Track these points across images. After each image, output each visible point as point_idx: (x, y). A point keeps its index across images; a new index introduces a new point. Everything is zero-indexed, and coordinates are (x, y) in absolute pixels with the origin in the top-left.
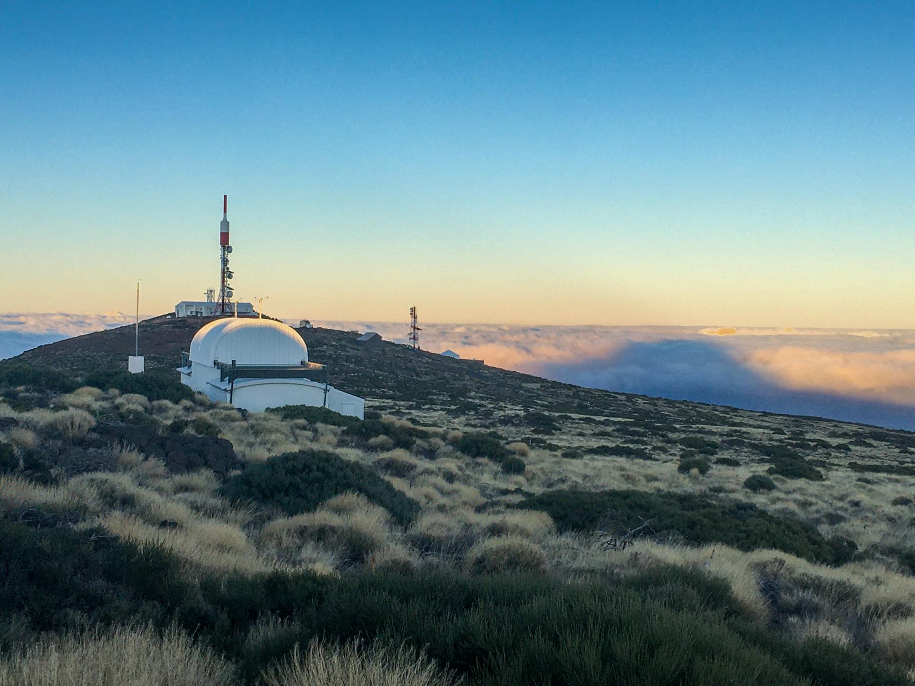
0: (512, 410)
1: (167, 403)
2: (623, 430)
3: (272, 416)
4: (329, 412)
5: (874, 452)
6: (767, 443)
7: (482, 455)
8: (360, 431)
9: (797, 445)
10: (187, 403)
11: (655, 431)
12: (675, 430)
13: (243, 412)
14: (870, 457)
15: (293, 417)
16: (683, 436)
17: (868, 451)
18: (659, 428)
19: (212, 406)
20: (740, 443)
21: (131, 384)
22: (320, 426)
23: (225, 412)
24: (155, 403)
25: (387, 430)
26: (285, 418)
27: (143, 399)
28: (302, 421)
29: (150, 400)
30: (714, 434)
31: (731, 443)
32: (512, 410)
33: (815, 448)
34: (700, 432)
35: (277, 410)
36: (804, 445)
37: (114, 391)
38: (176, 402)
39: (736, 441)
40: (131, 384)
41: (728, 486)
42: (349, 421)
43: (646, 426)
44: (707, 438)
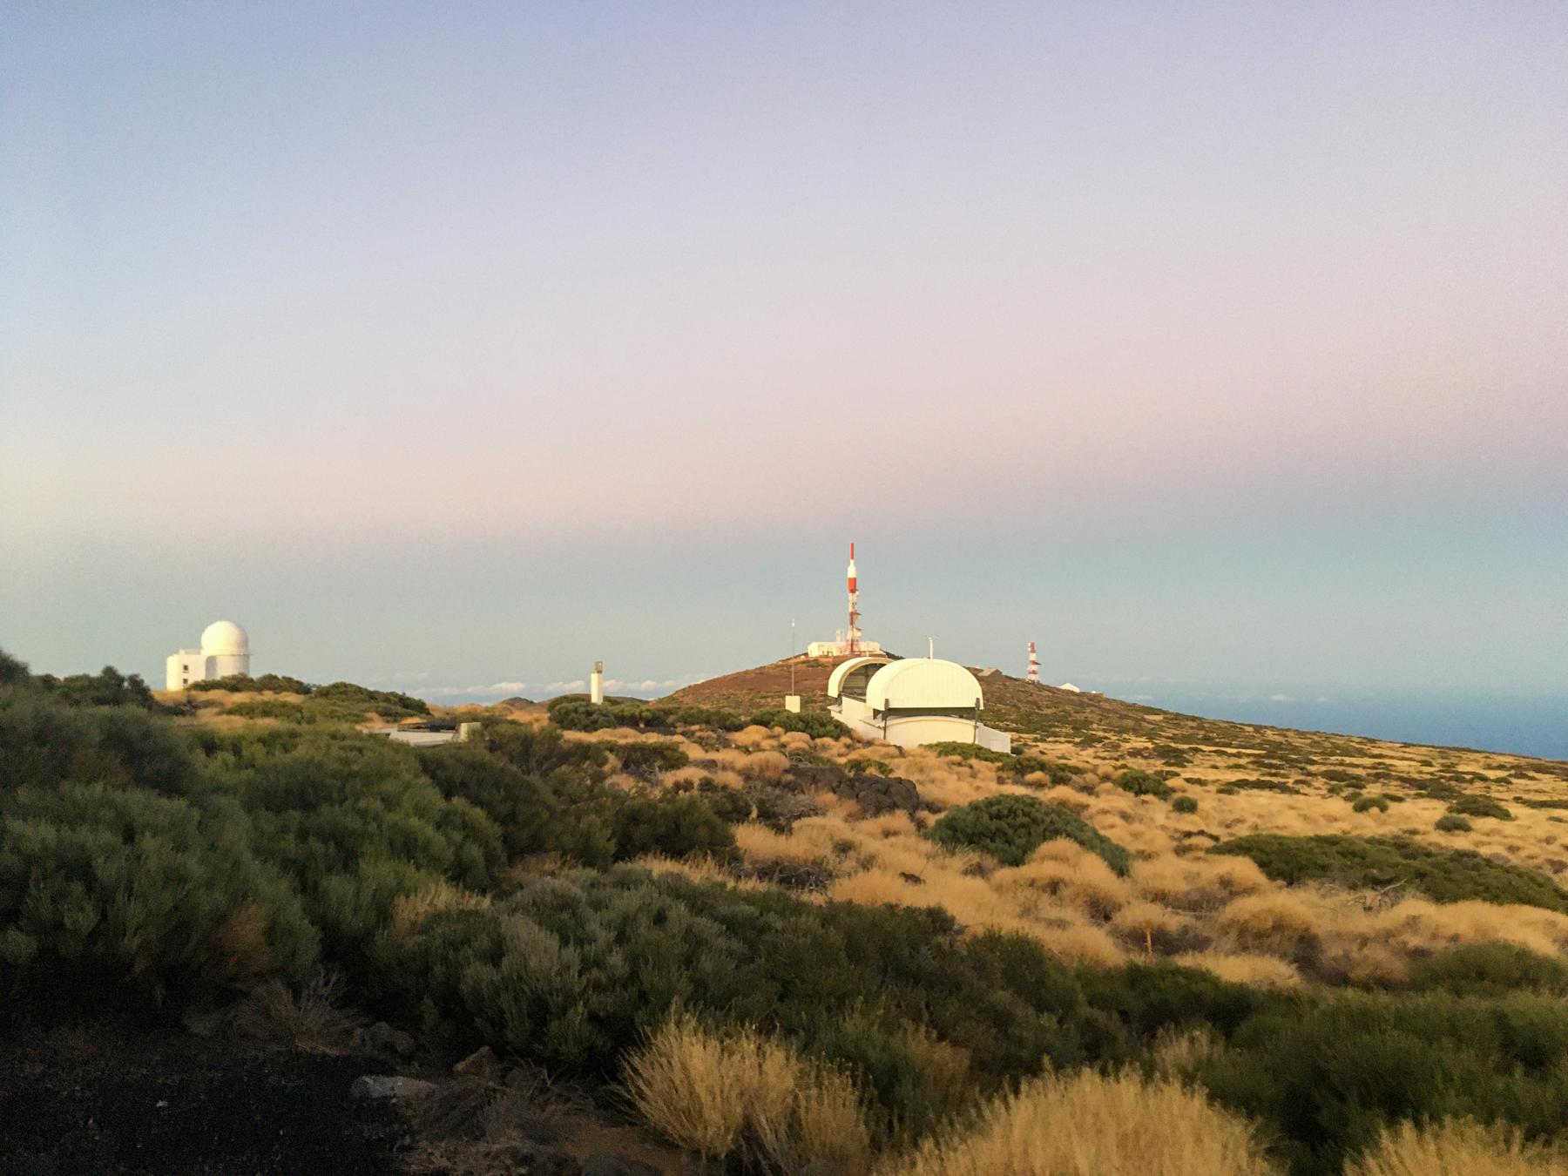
0: (1140, 743)
1: (828, 740)
2: (1258, 762)
3: (928, 753)
4: (980, 748)
5: (1540, 786)
6: (1416, 776)
7: (1146, 792)
8: (1017, 765)
9: (1451, 779)
10: (845, 740)
11: (1292, 764)
12: (1313, 763)
13: (899, 748)
14: (1536, 791)
15: (947, 754)
16: (1324, 768)
17: (1531, 785)
18: (1297, 761)
19: (869, 743)
20: (1387, 776)
21: (791, 724)
22: (973, 761)
23: (885, 750)
24: (818, 741)
25: (1042, 767)
26: (940, 755)
27: (806, 736)
28: (957, 758)
29: (813, 738)
30: (1357, 766)
31: (1378, 776)
32: (1140, 743)
33: (1471, 782)
34: (1342, 764)
35: (930, 747)
36: (1459, 778)
37: (778, 730)
38: (837, 738)
39: (1382, 774)
40: (791, 724)
41: (1422, 828)
42: (998, 757)
43: (1281, 758)
44: (1351, 771)
